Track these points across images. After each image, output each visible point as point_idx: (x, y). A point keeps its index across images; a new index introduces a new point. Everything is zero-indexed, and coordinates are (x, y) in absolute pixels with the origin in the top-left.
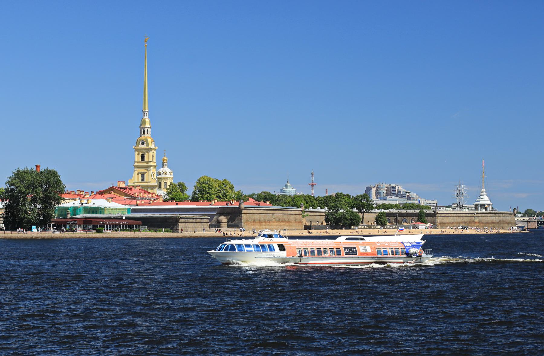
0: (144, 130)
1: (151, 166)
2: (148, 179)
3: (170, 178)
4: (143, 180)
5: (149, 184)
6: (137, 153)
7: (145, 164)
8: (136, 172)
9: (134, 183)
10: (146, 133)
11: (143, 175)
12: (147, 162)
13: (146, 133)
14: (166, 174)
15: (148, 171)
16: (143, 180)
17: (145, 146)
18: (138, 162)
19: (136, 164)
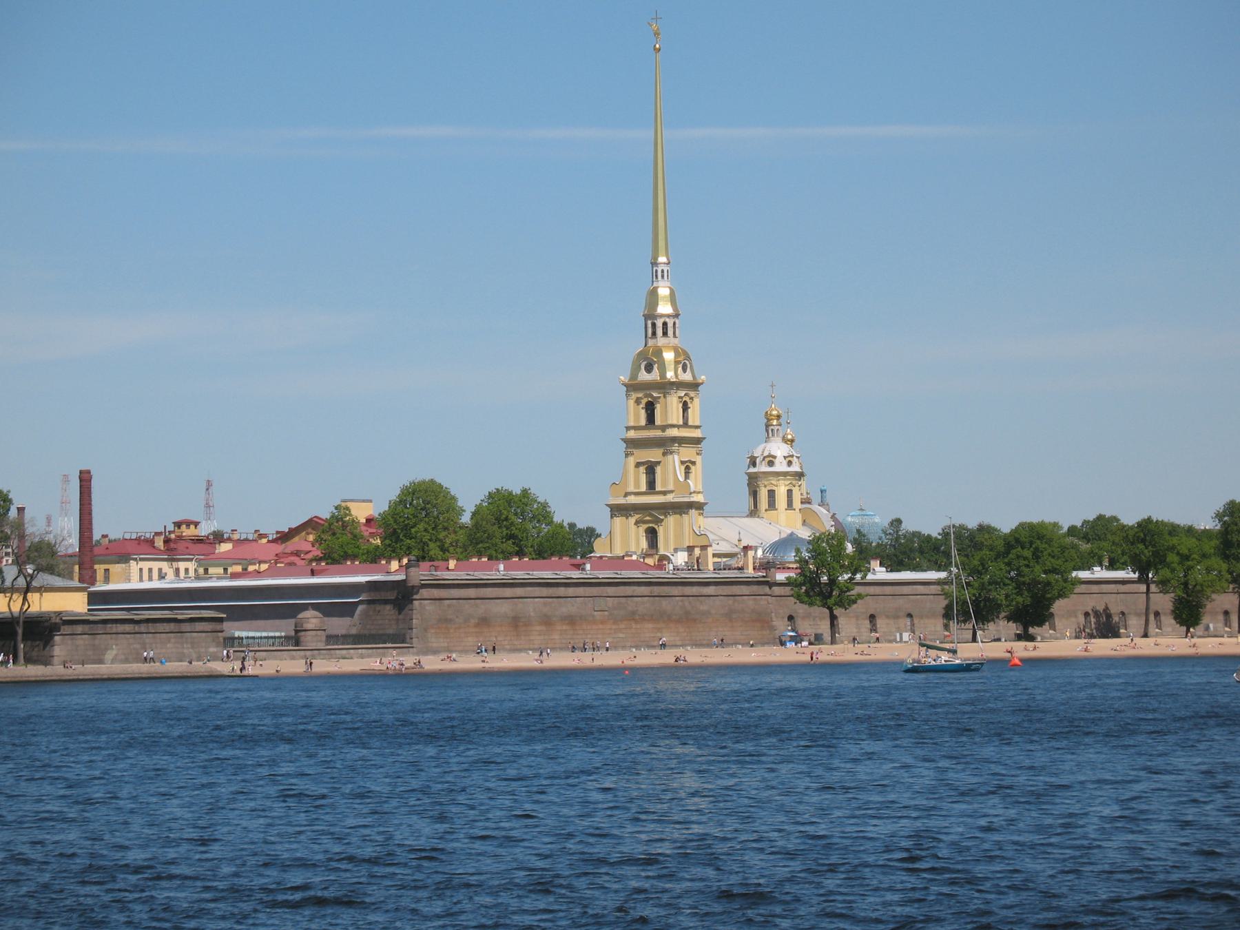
0: (654, 325)
1: (674, 440)
2: (664, 483)
3: (785, 474)
4: (651, 484)
5: (670, 498)
6: (634, 395)
7: (658, 433)
8: (632, 461)
9: (626, 495)
10: (659, 332)
11: (651, 469)
12: (664, 428)
13: (659, 332)
14: (771, 464)
15: (664, 454)
16: (651, 484)
17: (655, 376)
18: (635, 428)
19: (632, 434)
